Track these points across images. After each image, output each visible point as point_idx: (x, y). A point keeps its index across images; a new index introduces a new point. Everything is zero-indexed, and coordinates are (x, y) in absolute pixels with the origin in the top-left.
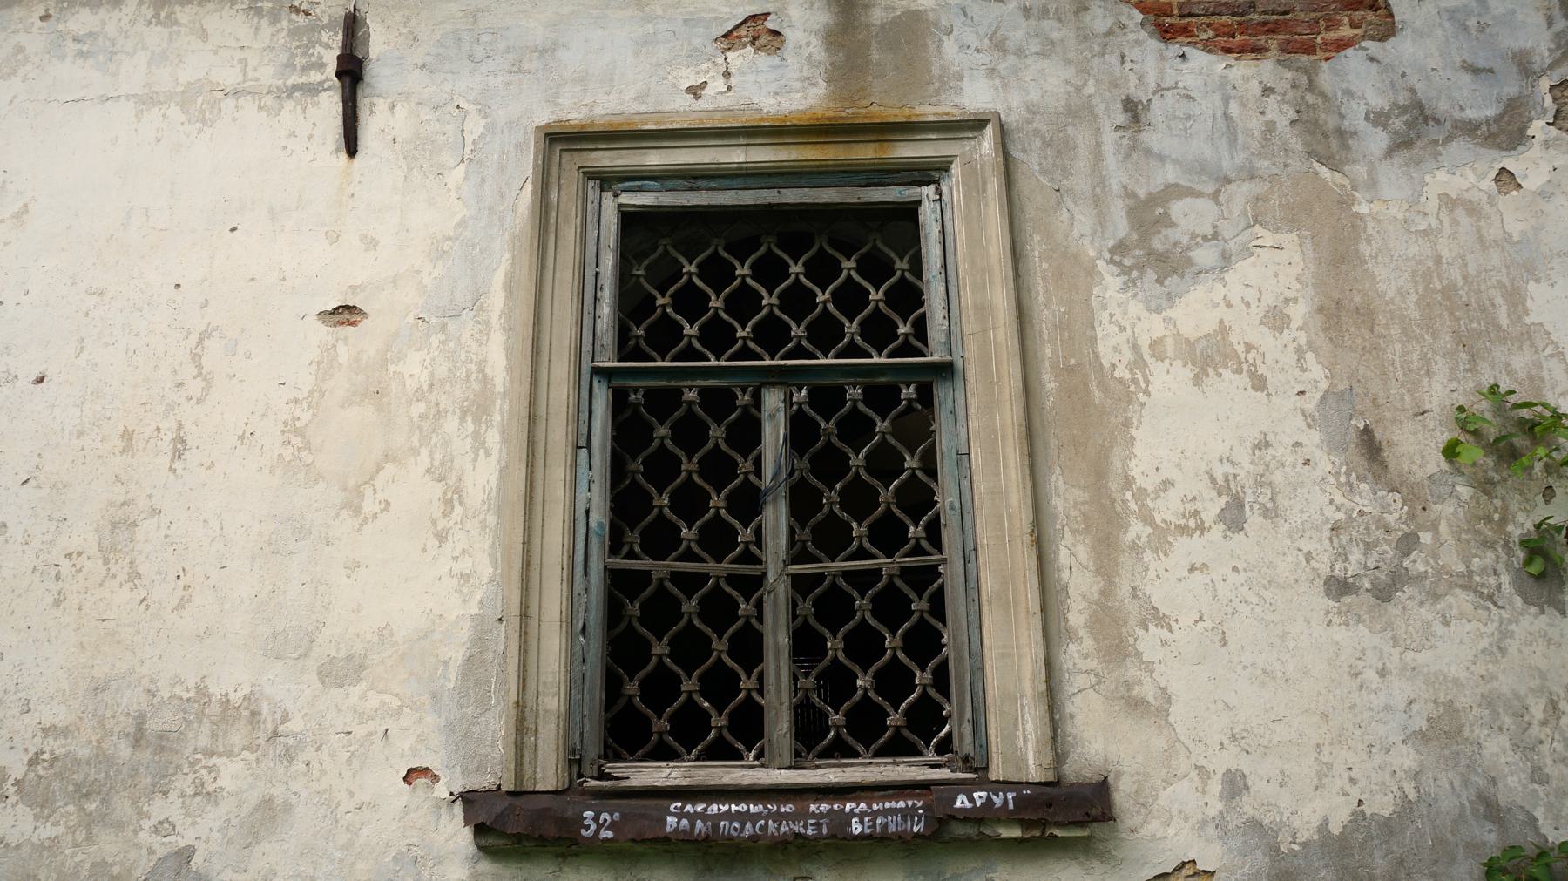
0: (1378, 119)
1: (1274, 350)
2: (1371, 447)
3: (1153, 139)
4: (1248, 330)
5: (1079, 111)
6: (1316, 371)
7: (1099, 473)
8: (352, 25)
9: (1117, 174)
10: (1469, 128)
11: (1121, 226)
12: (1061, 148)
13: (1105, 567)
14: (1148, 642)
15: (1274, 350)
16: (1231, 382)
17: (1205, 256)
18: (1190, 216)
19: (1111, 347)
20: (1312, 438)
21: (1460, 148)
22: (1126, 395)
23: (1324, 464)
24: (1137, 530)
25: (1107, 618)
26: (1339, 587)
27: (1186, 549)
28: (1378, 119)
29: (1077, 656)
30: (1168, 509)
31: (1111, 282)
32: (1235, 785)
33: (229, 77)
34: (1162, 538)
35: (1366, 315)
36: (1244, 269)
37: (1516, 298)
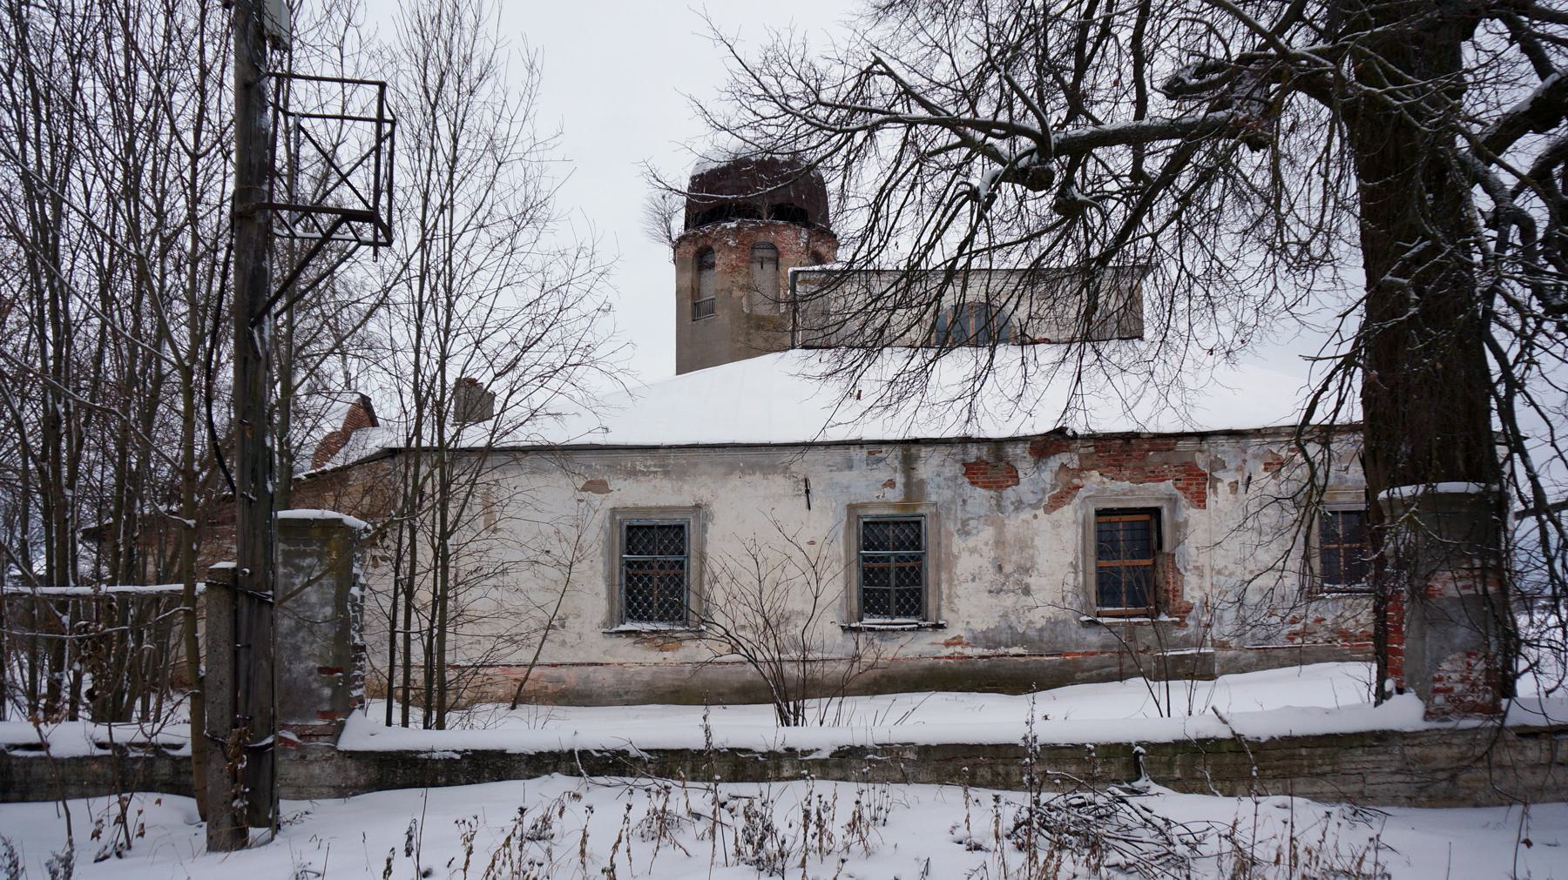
0: (1012, 503)
1: (985, 550)
2: (1000, 568)
3: (968, 508)
4: (981, 545)
5: (953, 501)
6: (992, 553)
7: (950, 571)
8: (806, 481)
9: (959, 514)
10: (1030, 505)
11: (959, 526)
12: (949, 509)
13: (950, 587)
14: (956, 601)
15: (985, 550)
16: (976, 555)
17: (974, 532)
18: (973, 523)
19: (955, 550)
20: (990, 566)
21: (1028, 509)
22: (956, 558)
23: (991, 570)
24: (956, 582)
25: (949, 596)
26: (990, 592)
27: (965, 585)
28: (1012, 503)
29: (944, 603)
30: (962, 578)
31: (956, 536)
32: (968, 623)
33: (782, 492)
34: (960, 584)
35: (1003, 543)
36: (981, 534)
37: (1032, 540)
